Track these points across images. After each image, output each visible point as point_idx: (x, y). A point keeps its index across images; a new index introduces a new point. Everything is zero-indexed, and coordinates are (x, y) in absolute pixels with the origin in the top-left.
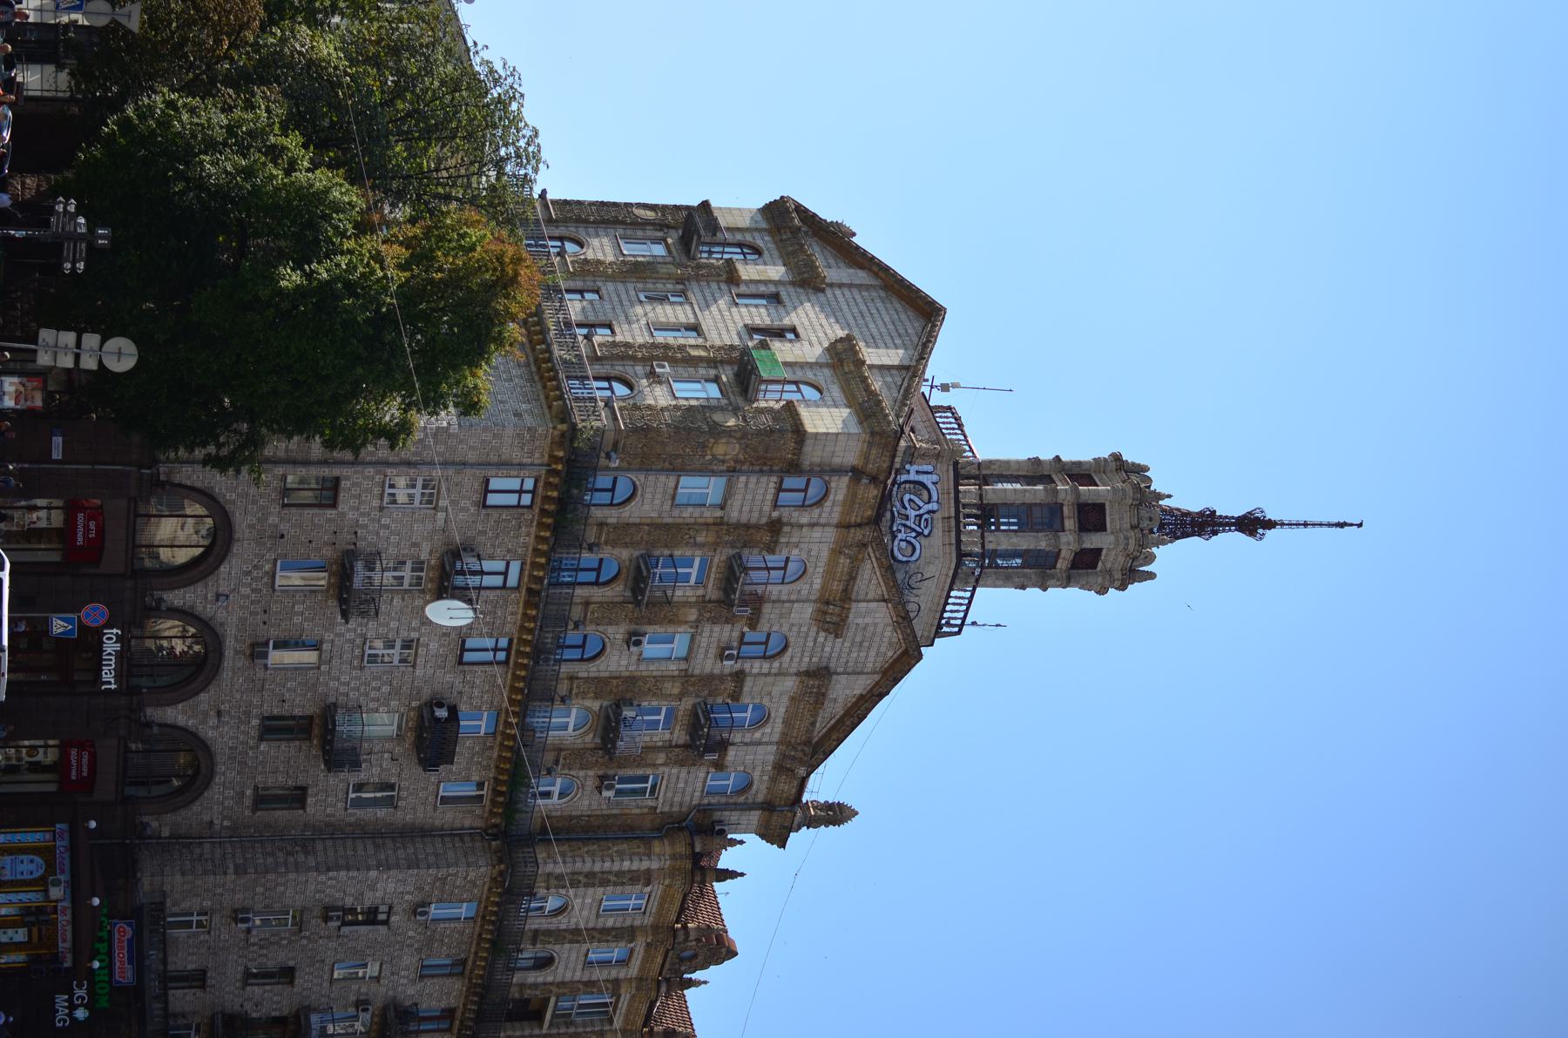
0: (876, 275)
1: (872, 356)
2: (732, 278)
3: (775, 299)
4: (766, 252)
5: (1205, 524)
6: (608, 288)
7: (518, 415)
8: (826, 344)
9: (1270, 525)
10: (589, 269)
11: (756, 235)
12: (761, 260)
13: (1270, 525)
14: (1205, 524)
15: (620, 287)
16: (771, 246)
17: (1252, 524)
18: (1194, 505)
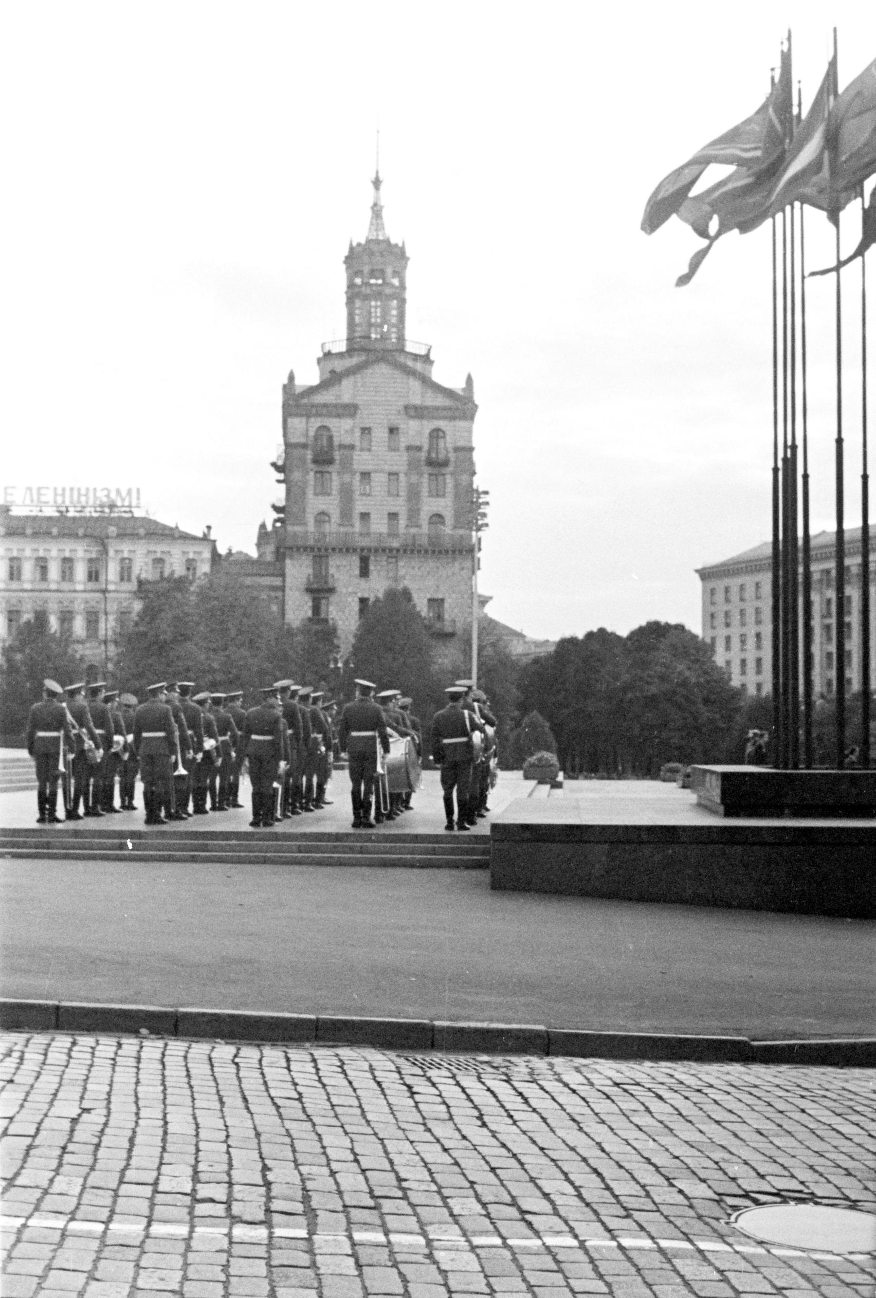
0: (348, 375)
1: (416, 400)
2: (352, 447)
3: (366, 431)
4: (325, 424)
5: (377, 211)
6: (359, 507)
7: (463, 569)
8: (404, 417)
9: (377, 172)
10: (346, 514)
11: (310, 425)
12: (333, 429)
13: (377, 172)
14: (377, 211)
15: (357, 503)
16: (319, 419)
17: (377, 183)
18: (369, 214)
